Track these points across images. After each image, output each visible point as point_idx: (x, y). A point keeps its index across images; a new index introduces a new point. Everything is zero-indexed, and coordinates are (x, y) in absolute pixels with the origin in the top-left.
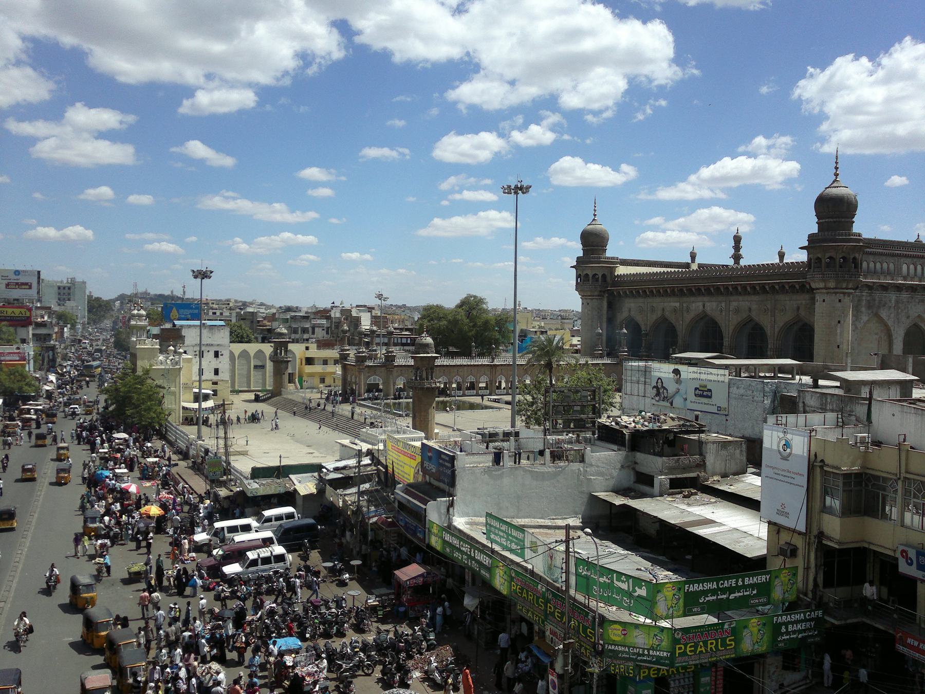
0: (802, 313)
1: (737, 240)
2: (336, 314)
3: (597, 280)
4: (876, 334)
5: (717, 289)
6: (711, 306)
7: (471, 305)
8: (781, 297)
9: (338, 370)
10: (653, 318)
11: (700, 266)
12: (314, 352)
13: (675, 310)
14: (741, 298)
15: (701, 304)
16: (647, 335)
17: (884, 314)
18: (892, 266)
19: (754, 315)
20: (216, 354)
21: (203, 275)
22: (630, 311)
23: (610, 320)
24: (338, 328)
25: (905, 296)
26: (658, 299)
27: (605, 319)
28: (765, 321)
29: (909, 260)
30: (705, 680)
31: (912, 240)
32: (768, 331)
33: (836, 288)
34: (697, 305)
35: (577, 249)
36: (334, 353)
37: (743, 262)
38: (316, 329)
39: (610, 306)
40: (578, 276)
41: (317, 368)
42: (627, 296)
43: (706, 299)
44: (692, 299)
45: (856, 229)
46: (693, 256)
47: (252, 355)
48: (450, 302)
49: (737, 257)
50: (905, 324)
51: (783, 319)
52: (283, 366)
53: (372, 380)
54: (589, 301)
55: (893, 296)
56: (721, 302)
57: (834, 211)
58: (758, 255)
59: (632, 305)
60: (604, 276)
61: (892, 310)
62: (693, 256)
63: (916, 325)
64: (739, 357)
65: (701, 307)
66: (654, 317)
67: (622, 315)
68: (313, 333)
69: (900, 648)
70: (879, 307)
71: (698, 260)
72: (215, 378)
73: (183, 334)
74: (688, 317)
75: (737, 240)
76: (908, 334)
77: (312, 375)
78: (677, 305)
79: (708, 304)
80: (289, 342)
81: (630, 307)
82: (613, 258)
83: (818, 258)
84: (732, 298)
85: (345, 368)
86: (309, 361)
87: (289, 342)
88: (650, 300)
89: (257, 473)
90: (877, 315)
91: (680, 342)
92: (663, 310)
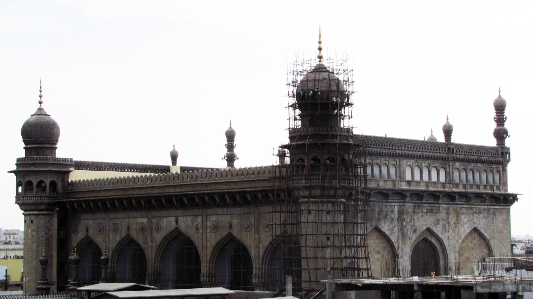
1: (230, 136)
3: (44, 189)
4: (378, 253)
5: (191, 198)
6: (186, 222)
10: (115, 239)
11: (183, 169)
13: (143, 229)
14: (219, 211)
15: (173, 219)
16: (107, 260)
17: (385, 228)
18: (393, 171)
19: (235, 232)
22: (87, 230)
23: (63, 244)
25: (409, 206)
26: (121, 215)
27: (55, 243)
28: (248, 240)
29: (411, 162)
32: (253, 253)
33: (322, 196)
34: (168, 222)
35: (19, 151)
37: (238, 165)
40: (18, 184)
42: (83, 211)
43: (179, 212)
44: (163, 213)
45: (345, 124)
46: (174, 157)
49: (231, 159)
50: (413, 238)
54: (33, 218)
56: (196, 216)
57: (320, 100)
59: (91, 222)
60: (53, 184)
61: (396, 223)
62: (174, 157)
63: (425, 240)
64: (161, 288)
65: (173, 224)
66: (118, 238)
67: (77, 238)
70: (379, 220)
71: (182, 162)
74: (159, 237)
75: (230, 136)
76: (416, 251)
78: (145, 220)
79: (181, 219)
82: (65, 160)
83: (301, 159)
84: (209, 211)
88: (112, 215)
90: (377, 229)
91: (150, 270)
92: (129, 228)
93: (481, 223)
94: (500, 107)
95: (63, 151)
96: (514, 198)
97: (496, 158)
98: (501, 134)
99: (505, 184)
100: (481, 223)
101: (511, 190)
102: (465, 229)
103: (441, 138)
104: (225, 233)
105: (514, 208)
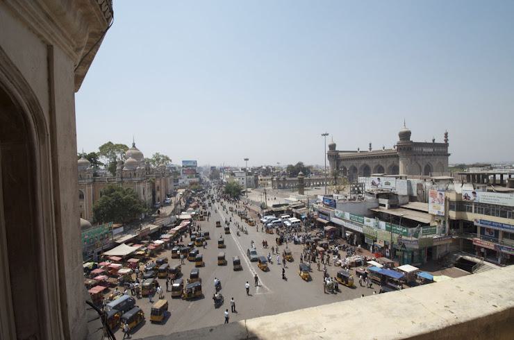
0: (395, 163)
1: (370, 144)
2: (264, 168)
6: (367, 162)
7: (300, 164)
8: (388, 159)
12: (262, 178)
17: (419, 162)
21: (247, 160)
23: (338, 168)
25: (424, 157)
28: (384, 165)
30: (423, 251)
31: (424, 142)
32: (385, 168)
34: (363, 162)
35: (328, 149)
39: (337, 163)
45: (411, 140)
48: (294, 164)
49: (370, 149)
51: (388, 165)
55: (421, 157)
58: (377, 147)
67: (340, 166)
69: (474, 243)
74: (360, 165)
75: (370, 144)
76: (426, 167)
81: (343, 163)
85: (273, 181)
89: (274, 206)
93: (441, 161)
94: (446, 134)
95: (337, 149)
96: (450, 155)
97: (446, 145)
98: (446, 140)
99: (447, 151)
100: (441, 161)
101: (449, 152)
102: (437, 162)
103: (432, 142)
104: (377, 164)
105: (449, 157)
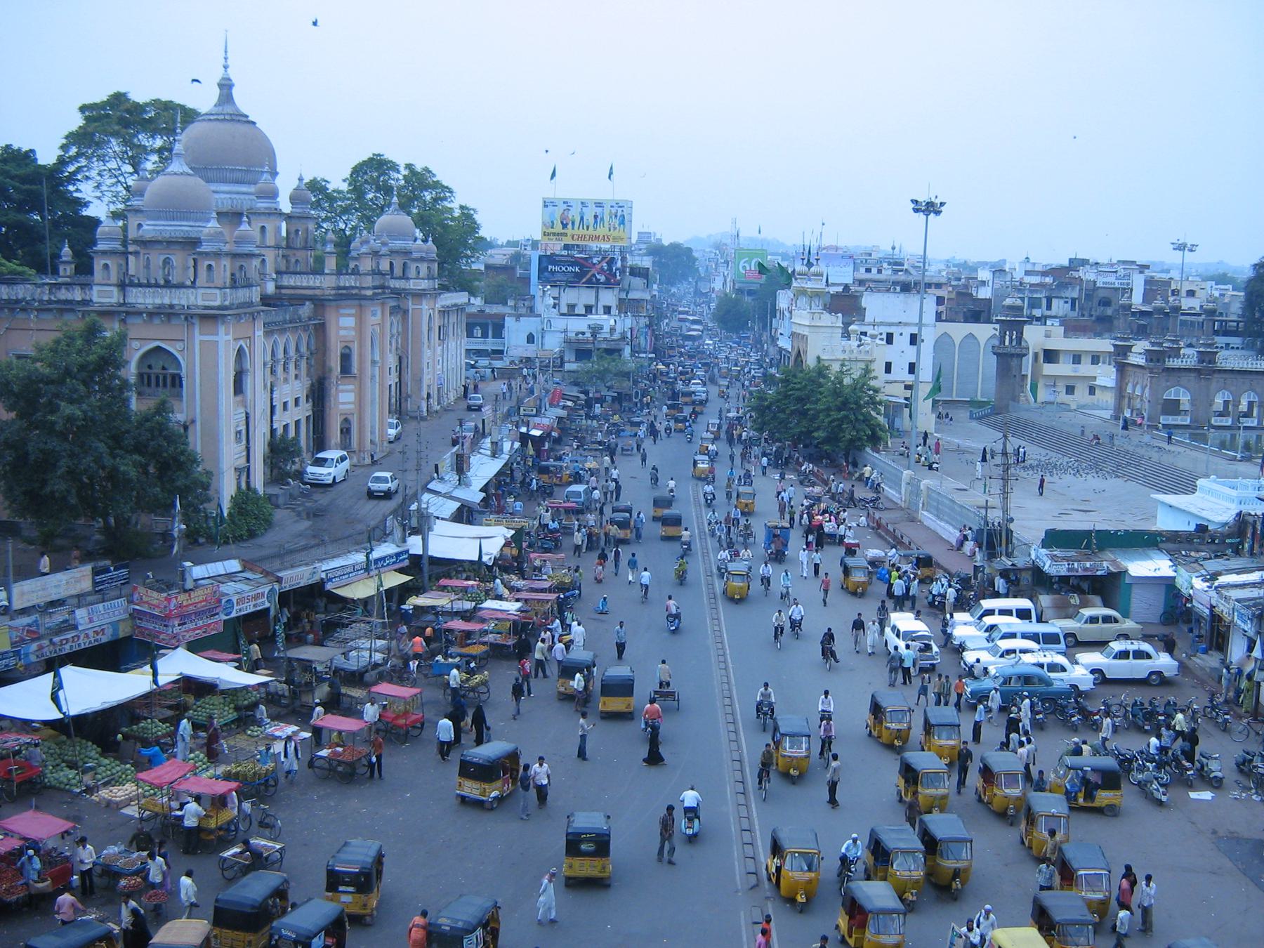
9: (1106, 376)
12: (1059, 342)
20: (914, 339)
21: (930, 208)
24: (1092, 302)
36: (1104, 345)
38: (1055, 302)
41: (1062, 368)
47: (957, 343)
52: (1014, 362)
53: (1171, 394)
68: (1049, 307)
72: (910, 379)
73: (863, 305)
77: (1055, 378)
80: (1025, 322)
85: (1122, 368)
86: (1051, 356)
87: (1025, 322)
89: (1054, 539)
